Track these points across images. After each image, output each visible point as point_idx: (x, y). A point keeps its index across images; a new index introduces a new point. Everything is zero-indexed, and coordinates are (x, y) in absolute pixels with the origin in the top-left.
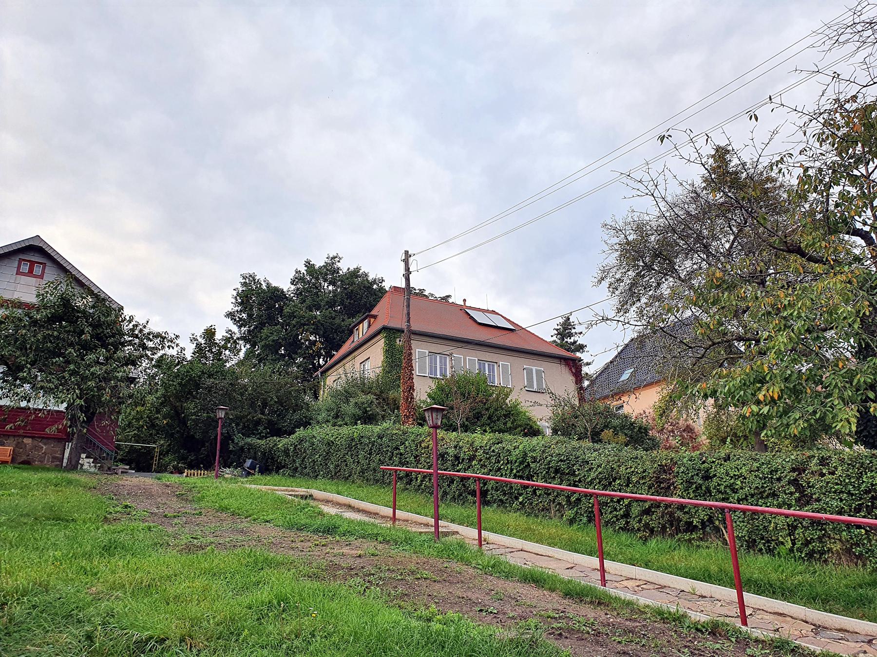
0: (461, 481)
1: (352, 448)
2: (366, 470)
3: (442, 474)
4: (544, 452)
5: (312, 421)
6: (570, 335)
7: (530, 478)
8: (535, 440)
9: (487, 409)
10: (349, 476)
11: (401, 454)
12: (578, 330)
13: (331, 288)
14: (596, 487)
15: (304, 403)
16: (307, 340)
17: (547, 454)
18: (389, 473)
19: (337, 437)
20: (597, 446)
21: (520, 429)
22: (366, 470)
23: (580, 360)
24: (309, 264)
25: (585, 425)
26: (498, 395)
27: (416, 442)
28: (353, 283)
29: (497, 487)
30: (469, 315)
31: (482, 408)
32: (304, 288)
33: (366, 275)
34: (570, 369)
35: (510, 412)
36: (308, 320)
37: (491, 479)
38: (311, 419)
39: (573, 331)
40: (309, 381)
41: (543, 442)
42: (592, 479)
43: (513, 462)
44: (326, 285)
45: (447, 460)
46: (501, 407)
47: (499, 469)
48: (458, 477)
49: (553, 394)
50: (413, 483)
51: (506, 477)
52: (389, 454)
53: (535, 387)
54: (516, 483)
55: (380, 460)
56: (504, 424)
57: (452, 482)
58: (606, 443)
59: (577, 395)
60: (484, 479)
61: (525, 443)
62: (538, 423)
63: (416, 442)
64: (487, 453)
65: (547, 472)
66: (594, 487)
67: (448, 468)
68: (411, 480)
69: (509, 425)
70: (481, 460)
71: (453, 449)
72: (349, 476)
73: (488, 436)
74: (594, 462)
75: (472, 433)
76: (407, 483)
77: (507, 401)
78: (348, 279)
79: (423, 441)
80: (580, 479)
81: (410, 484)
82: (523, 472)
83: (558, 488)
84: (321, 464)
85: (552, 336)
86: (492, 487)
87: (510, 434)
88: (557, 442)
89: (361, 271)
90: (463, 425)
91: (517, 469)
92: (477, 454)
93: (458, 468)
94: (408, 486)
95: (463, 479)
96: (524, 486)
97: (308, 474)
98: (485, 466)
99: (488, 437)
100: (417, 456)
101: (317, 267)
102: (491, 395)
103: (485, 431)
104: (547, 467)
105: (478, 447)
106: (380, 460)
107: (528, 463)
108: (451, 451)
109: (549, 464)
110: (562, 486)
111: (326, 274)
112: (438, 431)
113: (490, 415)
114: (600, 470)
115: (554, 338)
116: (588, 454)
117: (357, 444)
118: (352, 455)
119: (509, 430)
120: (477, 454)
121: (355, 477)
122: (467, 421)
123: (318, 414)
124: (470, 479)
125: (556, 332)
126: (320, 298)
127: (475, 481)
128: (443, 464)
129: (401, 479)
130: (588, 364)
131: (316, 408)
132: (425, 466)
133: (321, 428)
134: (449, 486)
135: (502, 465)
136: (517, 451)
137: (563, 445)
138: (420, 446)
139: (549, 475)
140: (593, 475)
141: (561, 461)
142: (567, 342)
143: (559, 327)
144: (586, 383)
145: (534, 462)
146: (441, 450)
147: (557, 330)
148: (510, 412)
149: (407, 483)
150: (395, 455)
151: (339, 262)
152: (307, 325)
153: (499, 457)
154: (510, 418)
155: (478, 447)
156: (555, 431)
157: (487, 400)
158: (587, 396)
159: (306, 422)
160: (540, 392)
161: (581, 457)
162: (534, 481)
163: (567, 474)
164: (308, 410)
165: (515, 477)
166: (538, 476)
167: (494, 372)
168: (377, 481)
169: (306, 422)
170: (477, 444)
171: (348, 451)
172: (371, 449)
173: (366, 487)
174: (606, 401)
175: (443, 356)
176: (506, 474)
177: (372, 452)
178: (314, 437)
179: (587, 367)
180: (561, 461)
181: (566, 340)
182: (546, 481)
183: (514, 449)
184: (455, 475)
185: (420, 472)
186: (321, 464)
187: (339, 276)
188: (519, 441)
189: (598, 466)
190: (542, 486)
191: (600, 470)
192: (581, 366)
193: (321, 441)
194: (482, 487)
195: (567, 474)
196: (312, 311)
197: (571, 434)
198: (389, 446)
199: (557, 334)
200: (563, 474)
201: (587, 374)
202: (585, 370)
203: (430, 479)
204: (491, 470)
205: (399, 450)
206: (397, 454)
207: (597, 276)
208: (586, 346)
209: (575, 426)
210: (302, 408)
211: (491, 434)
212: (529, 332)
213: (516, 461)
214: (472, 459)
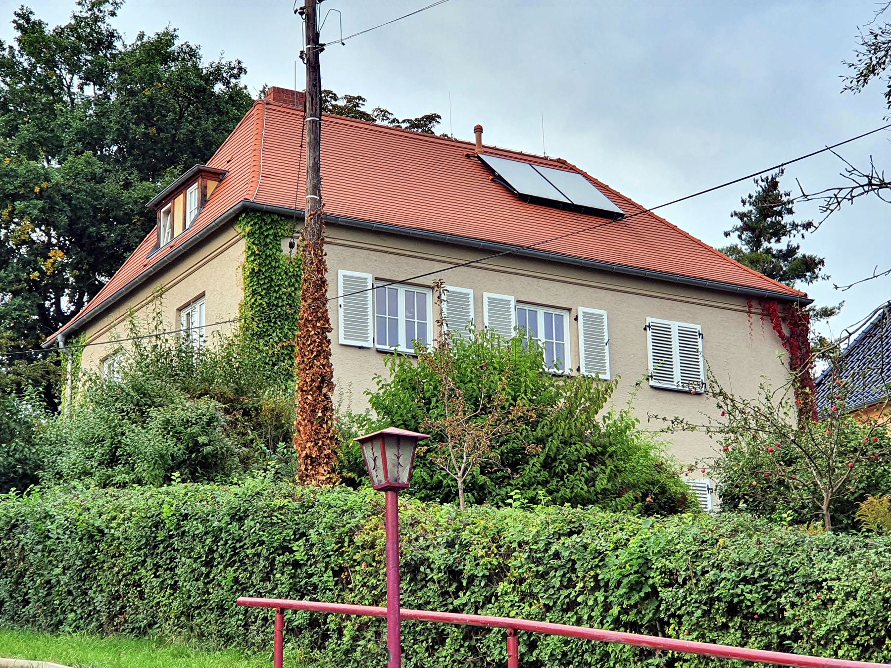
0: (465, 639)
1: (156, 547)
2: (197, 608)
3: (411, 617)
4: (697, 556)
5: (40, 473)
6: (779, 231)
7: (657, 627)
8: (672, 526)
9: (540, 441)
10: (150, 625)
11: (296, 565)
12: (798, 217)
13: (90, 90)
14: (840, 653)
15: (18, 422)
16: (24, 242)
17: (705, 563)
18: (261, 616)
19: (114, 518)
20: (848, 541)
21: (630, 495)
22: (197, 608)
23: (805, 301)
24: (28, 20)
25: (816, 485)
26: (573, 402)
27: (338, 531)
28: (152, 78)
29: (565, 654)
30: (491, 171)
31: (527, 437)
32: (13, 91)
33: (193, 54)
34: (777, 328)
35: (605, 447)
36: (24, 185)
37: (548, 633)
38: (38, 467)
39: (787, 219)
40: (30, 360)
41: (695, 530)
42: (829, 631)
43: (612, 584)
44: (77, 81)
45: (425, 580)
46: (580, 435)
47: (572, 605)
48: (457, 626)
49: (726, 398)
50: (331, 644)
51: (591, 627)
52: (262, 563)
53: (677, 376)
54: (617, 642)
55: (236, 580)
56: (587, 482)
57: (441, 639)
58: (869, 531)
59: (793, 399)
60: (529, 632)
61: (645, 533)
62: (683, 479)
63: (338, 531)
64: (538, 562)
65: (705, 613)
66: (836, 654)
67: (428, 603)
68: (325, 636)
69: (602, 483)
70: (521, 581)
71: (443, 551)
72: (150, 625)
73: (542, 514)
74: (836, 584)
75: (498, 507)
76: (315, 645)
77: (598, 418)
78: (138, 64)
79: (359, 528)
80: (796, 630)
81: (321, 647)
82: (639, 612)
83: (735, 655)
84: (70, 593)
85: (727, 234)
86: (552, 655)
87: (604, 509)
88: (735, 531)
89: (178, 43)
90: (472, 487)
91: (621, 604)
92: (512, 563)
93: (457, 602)
94: (316, 654)
95: (474, 631)
96: (642, 651)
97: (32, 620)
98: (532, 595)
99: (543, 516)
100: (342, 569)
101: (49, 30)
102: (552, 402)
103: (534, 501)
104: (704, 597)
105: (515, 545)
106: (236, 580)
107: (653, 586)
108: (439, 556)
109: (712, 590)
110: (746, 650)
111: (77, 51)
112: (401, 501)
113: (548, 456)
114: (852, 605)
115: (734, 240)
116: (820, 562)
117: (171, 537)
118: (157, 566)
119: (602, 498)
120: (512, 563)
121: (167, 627)
122: (482, 473)
123: (60, 453)
124: (489, 631)
125: (739, 223)
126: (61, 120)
127: (505, 636)
128: (413, 592)
129: (296, 631)
130: (827, 313)
131: (51, 434)
132: (363, 598)
133: (67, 491)
134: (430, 650)
135: (581, 593)
136: (623, 555)
137: (750, 536)
138: (351, 541)
139: (710, 620)
140: (833, 619)
141: (746, 580)
142: (768, 251)
143: (748, 208)
144: (820, 367)
145: (670, 585)
146: (410, 552)
147: (742, 216)
148: (605, 447)
149: (315, 645)
150: (278, 566)
151: (113, 14)
152: (23, 198)
153: (573, 570)
154: (604, 464)
155: (515, 545)
156: (730, 500)
157: (541, 415)
158: (823, 404)
159: (25, 475)
160: (688, 393)
161: (801, 571)
162: (670, 637)
163: (762, 617)
164: (29, 441)
165: (617, 624)
166: (680, 624)
167: (560, 336)
168: (229, 639)
169: (25, 475)
170: (512, 534)
171: (146, 556)
172: (211, 551)
173: (197, 654)
174: (874, 416)
175: (554, 312)
176: (590, 618)
177: (213, 559)
178: (47, 516)
179: (824, 321)
180: (746, 580)
181: (765, 245)
182: (702, 637)
183: (616, 549)
184: (448, 619)
185: (348, 615)
186: (70, 593)
187: (114, 56)
188: (629, 528)
189: (848, 595)
190: (690, 650)
191: (852, 605)
192: (807, 318)
193: (70, 528)
194: (523, 655)
195: (762, 617)
196: (36, 159)
197: (773, 509)
198: (262, 543)
199: (742, 229)
200: (751, 616)
201: (822, 340)
202: (818, 329)
203: (378, 634)
204: (548, 608)
205: (291, 551)
206: (285, 564)
207: (856, 62)
208: (822, 262)
209: (787, 488)
210: (13, 436)
211: (552, 509)
212: (662, 221)
213: (619, 583)
214: (497, 574)
